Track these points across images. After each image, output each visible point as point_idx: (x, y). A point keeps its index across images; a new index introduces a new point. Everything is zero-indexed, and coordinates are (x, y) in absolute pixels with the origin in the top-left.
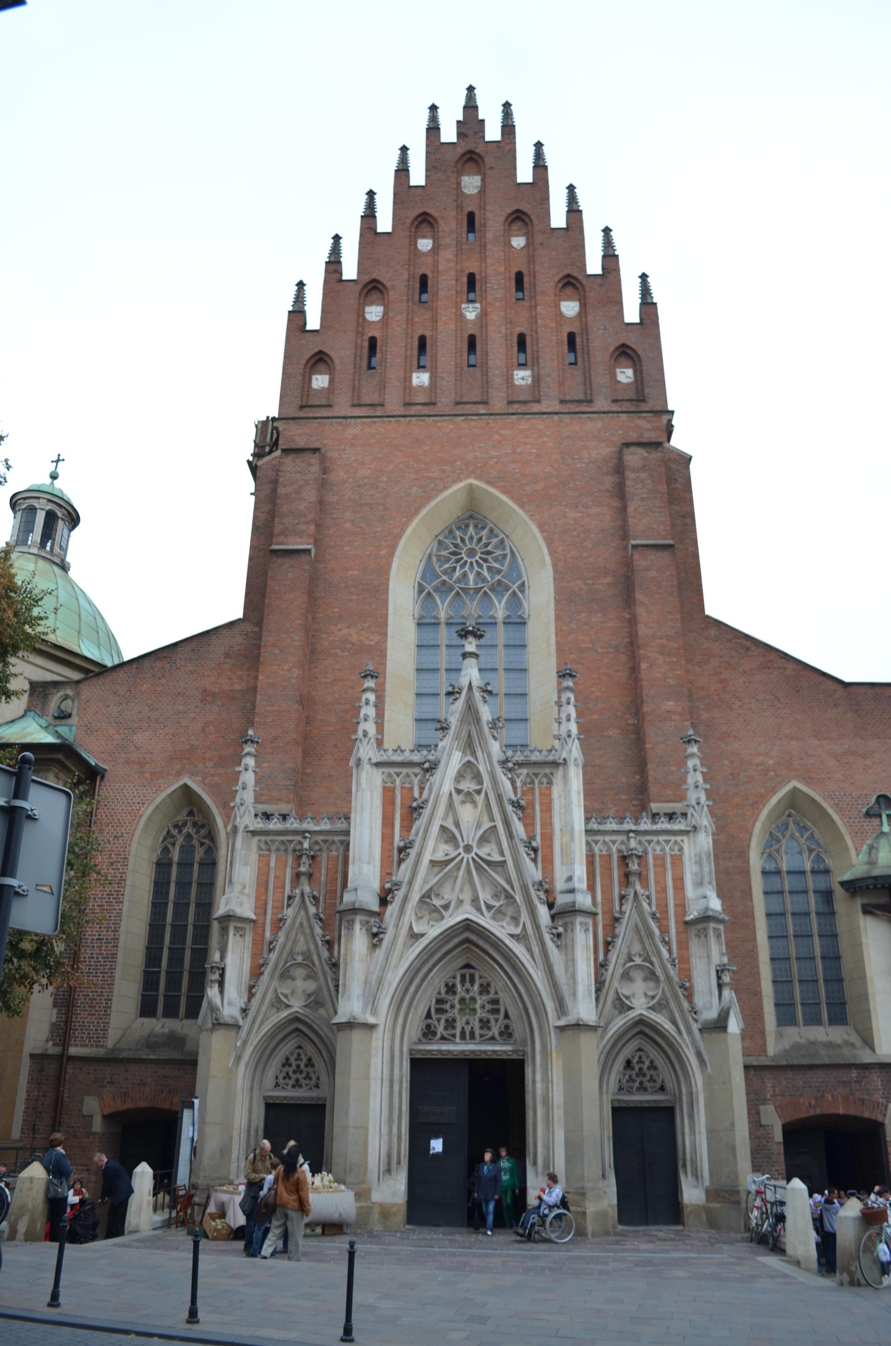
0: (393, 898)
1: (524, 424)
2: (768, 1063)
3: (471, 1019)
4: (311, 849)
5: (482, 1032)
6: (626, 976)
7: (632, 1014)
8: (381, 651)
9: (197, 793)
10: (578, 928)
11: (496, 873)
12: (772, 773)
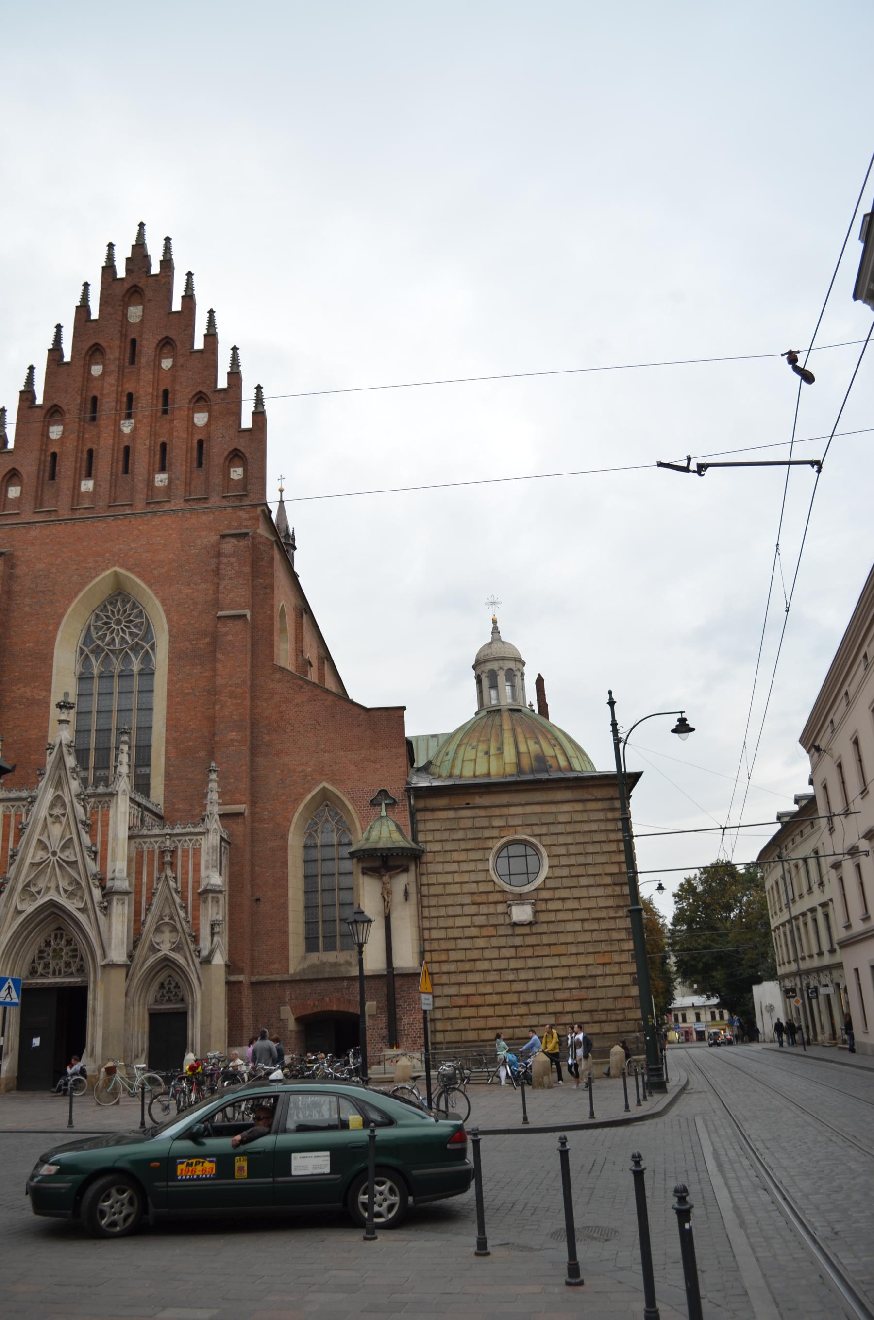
0: (4, 888)
1: (156, 521)
2: (288, 978)
3: (59, 962)
5: (66, 970)
6: (158, 930)
7: (160, 954)
8: (46, 703)
10: (114, 903)
11: (72, 868)
12: (310, 778)
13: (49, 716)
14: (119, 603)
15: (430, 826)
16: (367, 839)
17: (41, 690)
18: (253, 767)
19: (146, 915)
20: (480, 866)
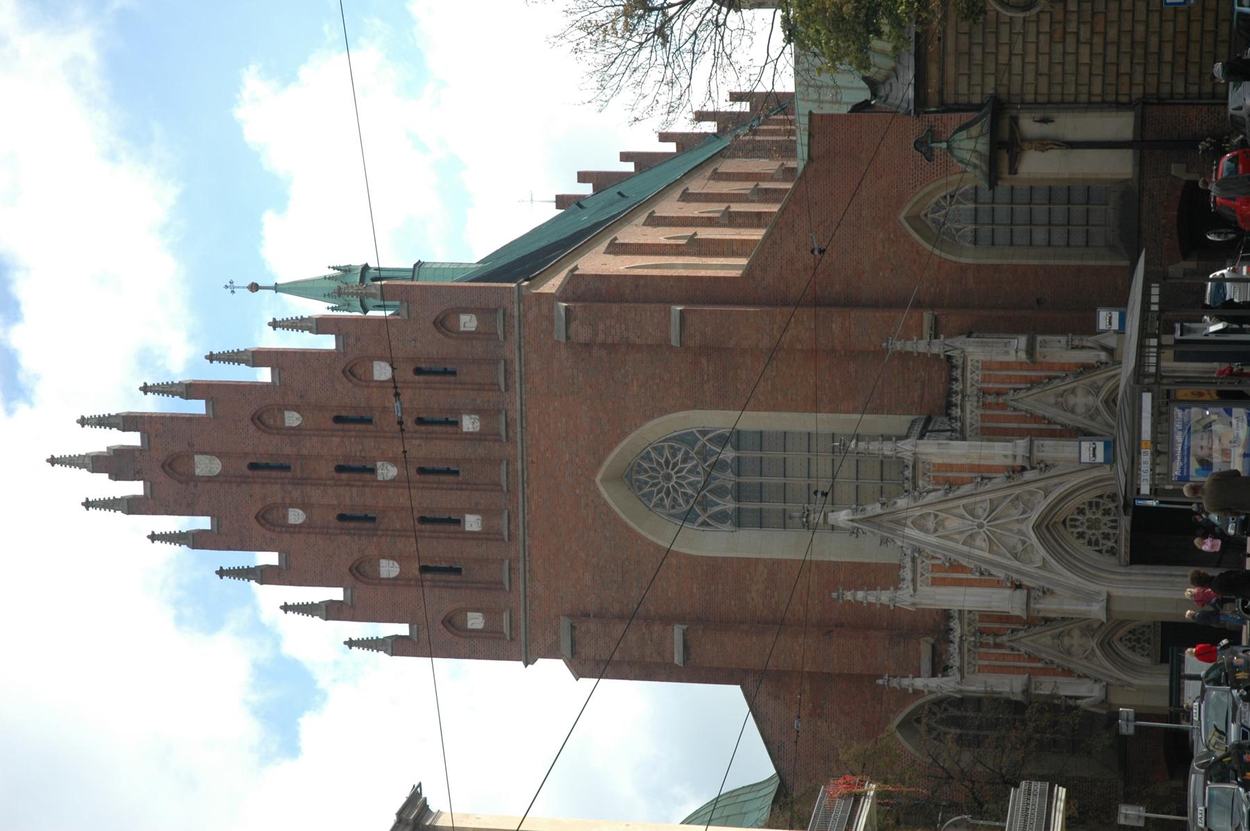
0: (1017, 581)
3: (1103, 522)
4: (974, 635)
5: (1113, 514)
6: (1073, 411)
7: (1101, 408)
9: (905, 717)
13: (791, 560)
14: (641, 477)
15: (963, 88)
16: (975, 166)
17: (756, 571)
18: (874, 305)
19: (1055, 423)
20: (1018, 28)
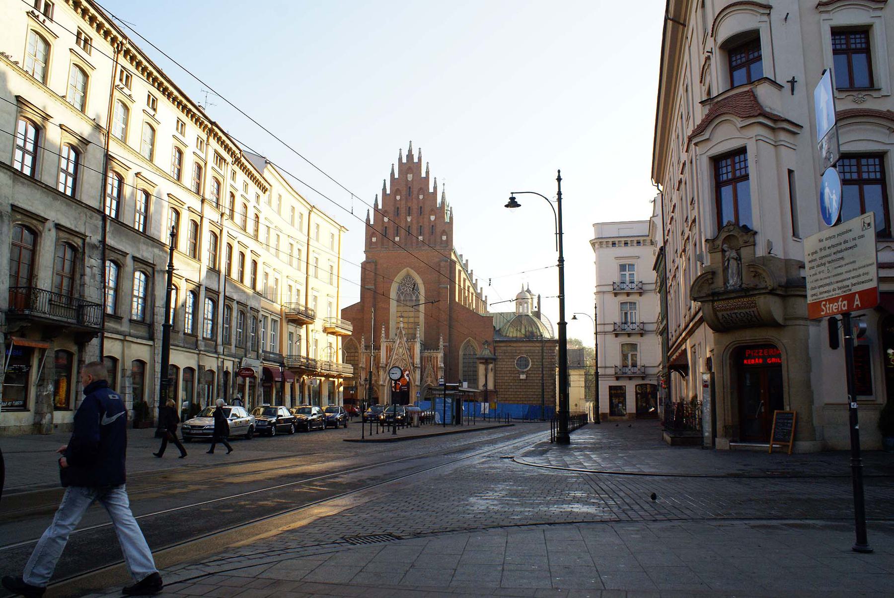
6: (427, 377)
